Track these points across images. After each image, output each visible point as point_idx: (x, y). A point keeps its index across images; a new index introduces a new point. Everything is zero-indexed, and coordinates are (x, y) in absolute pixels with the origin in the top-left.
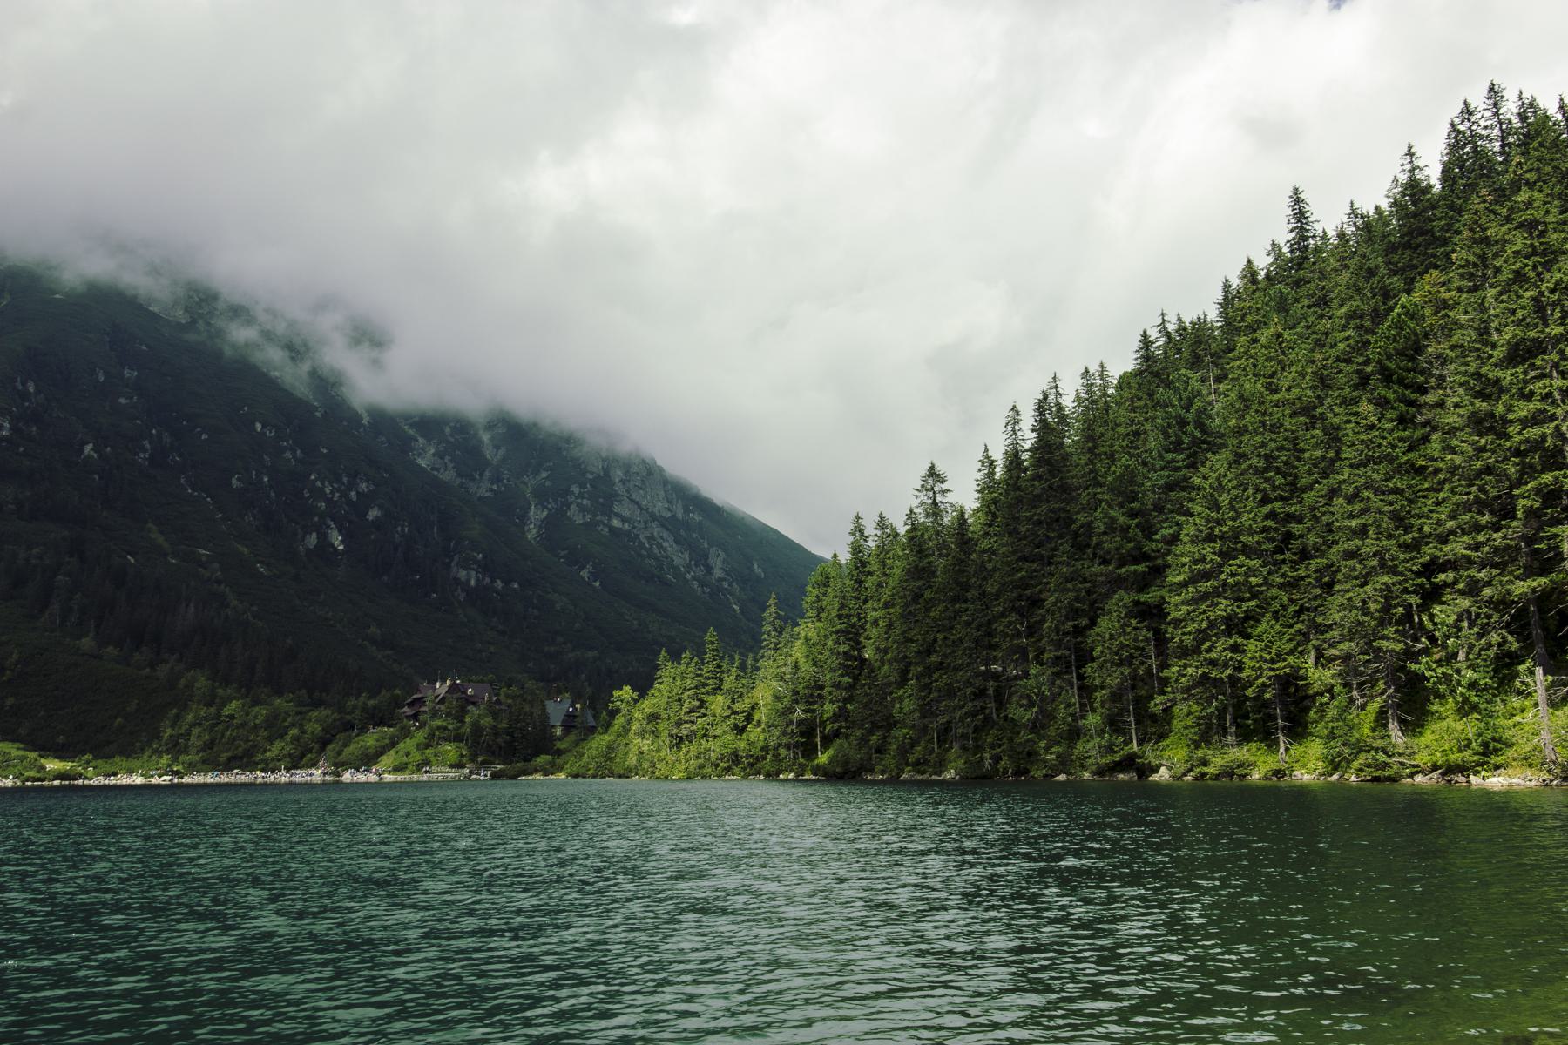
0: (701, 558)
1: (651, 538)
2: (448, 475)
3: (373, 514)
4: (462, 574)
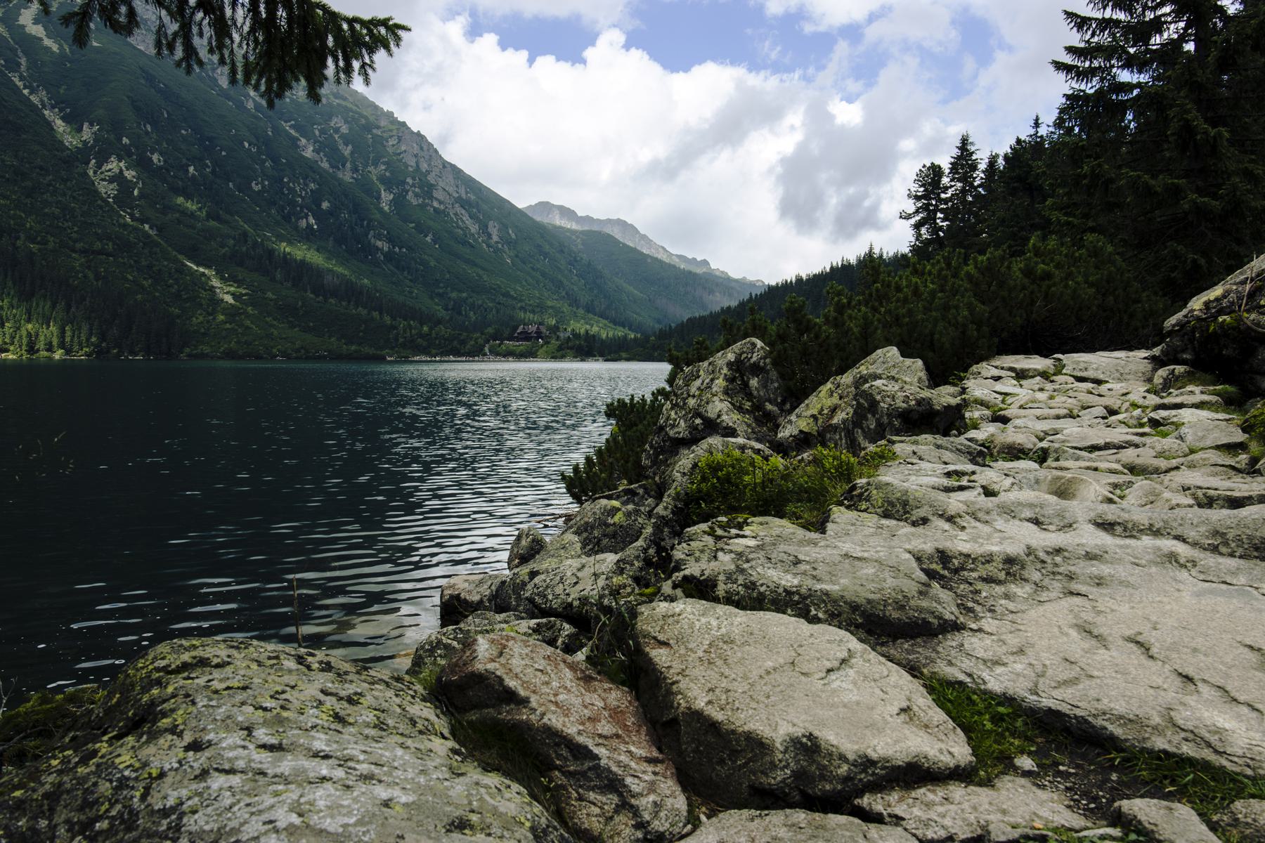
0: (484, 228)
1: (456, 214)
2: (325, 165)
3: (325, 205)
4: (379, 244)
